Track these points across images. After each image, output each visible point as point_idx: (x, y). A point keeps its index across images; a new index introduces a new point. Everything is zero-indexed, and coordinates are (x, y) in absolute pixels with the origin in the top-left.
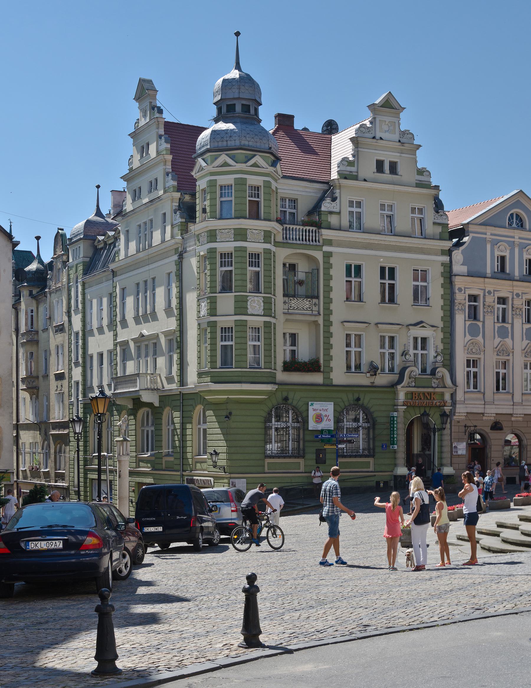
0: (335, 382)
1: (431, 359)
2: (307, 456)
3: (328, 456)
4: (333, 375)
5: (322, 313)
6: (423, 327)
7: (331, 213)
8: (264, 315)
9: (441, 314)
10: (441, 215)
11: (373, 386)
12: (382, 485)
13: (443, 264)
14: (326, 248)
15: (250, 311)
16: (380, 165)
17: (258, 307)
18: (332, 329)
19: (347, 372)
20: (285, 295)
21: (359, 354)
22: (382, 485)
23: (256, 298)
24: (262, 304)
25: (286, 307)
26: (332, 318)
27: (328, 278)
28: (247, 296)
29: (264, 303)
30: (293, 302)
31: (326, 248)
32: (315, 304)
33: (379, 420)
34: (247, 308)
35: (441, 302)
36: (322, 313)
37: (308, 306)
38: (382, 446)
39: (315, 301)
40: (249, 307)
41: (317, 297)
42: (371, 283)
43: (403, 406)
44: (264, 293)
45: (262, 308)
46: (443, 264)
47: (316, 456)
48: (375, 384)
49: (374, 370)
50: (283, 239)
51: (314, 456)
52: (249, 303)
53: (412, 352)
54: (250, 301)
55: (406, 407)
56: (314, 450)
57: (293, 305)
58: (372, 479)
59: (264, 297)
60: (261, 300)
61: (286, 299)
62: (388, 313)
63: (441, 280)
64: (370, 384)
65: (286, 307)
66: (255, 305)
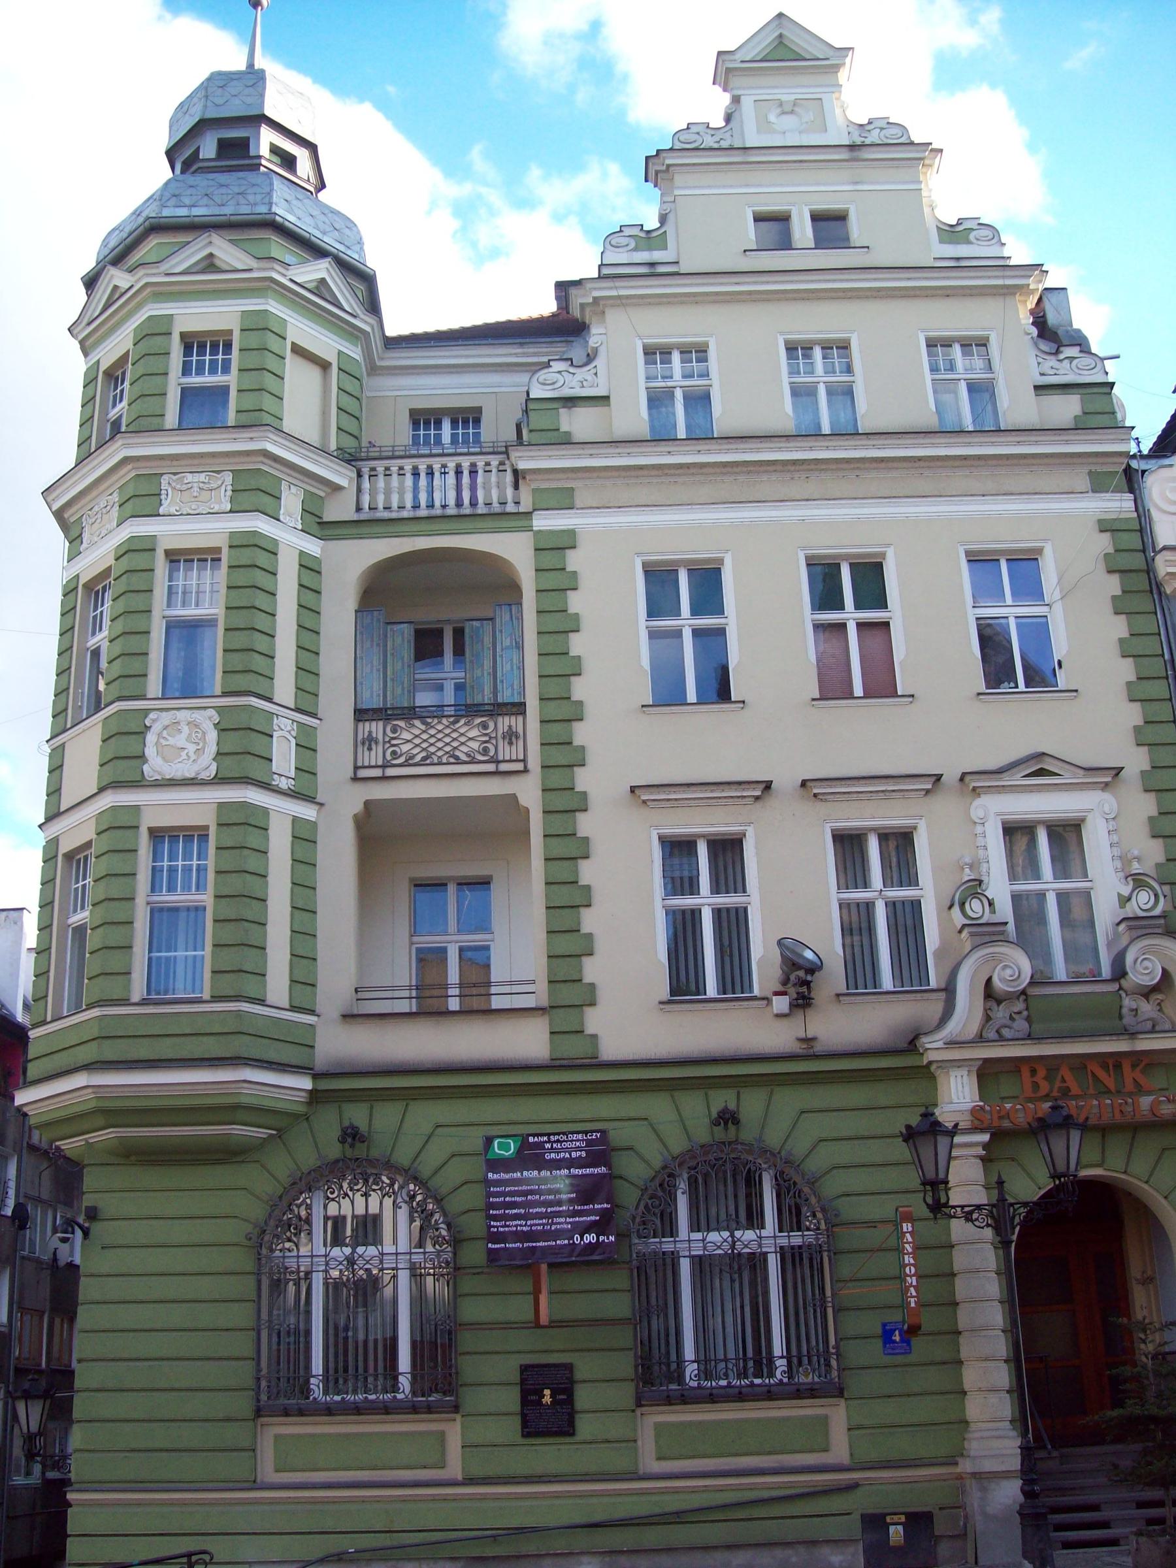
0: (610, 1050)
1: (1105, 912)
2: (472, 1399)
3: (583, 1397)
4: (594, 1021)
5: (534, 762)
6: (1041, 773)
7: (571, 402)
8: (220, 780)
9: (1133, 715)
10: (1072, 359)
11: (808, 1049)
12: (896, 1533)
13: (1106, 526)
14: (543, 522)
15: (155, 765)
16: (775, 222)
17: (192, 748)
18: (586, 825)
19: (669, 1002)
20: (361, 714)
21: (733, 925)
22: (896, 1533)
23: (182, 715)
24: (212, 735)
25: (375, 756)
26: (584, 780)
27: (560, 626)
28: (146, 712)
29: (222, 730)
30: (406, 736)
31: (543, 522)
32: (511, 736)
33: (850, 1210)
34: (142, 758)
35: (1126, 670)
36: (534, 762)
37: (475, 745)
38: (887, 1335)
39: (504, 723)
40: (150, 751)
41: (519, 708)
42: (768, 628)
43: (974, 1129)
44: (225, 694)
45: (212, 749)
46: (1106, 526)
47: (525, 1402)
48: (818, 1048)
49: (800, 979)
50: (359, 509)
51: (511, 1399)
52: (151, 738)
53: (999, 888)
54: (157, 727)
55: (986, 1137)
56: (509, 1369)
57: (405, 748)
58: (837, 1503)
59: (220, 710)
60: (207, 720)
61: (376, 728)
62: (863, 738)
63: (1113, 585)
64: (794, 1047)
65: (375, 756)
66: (180, 740)
